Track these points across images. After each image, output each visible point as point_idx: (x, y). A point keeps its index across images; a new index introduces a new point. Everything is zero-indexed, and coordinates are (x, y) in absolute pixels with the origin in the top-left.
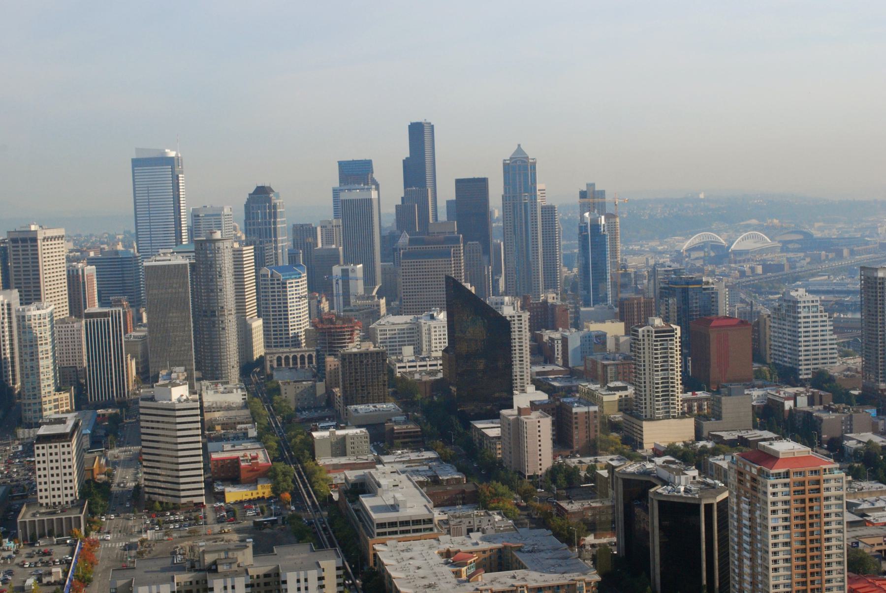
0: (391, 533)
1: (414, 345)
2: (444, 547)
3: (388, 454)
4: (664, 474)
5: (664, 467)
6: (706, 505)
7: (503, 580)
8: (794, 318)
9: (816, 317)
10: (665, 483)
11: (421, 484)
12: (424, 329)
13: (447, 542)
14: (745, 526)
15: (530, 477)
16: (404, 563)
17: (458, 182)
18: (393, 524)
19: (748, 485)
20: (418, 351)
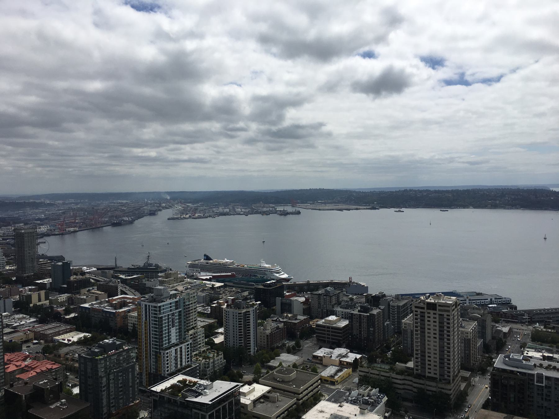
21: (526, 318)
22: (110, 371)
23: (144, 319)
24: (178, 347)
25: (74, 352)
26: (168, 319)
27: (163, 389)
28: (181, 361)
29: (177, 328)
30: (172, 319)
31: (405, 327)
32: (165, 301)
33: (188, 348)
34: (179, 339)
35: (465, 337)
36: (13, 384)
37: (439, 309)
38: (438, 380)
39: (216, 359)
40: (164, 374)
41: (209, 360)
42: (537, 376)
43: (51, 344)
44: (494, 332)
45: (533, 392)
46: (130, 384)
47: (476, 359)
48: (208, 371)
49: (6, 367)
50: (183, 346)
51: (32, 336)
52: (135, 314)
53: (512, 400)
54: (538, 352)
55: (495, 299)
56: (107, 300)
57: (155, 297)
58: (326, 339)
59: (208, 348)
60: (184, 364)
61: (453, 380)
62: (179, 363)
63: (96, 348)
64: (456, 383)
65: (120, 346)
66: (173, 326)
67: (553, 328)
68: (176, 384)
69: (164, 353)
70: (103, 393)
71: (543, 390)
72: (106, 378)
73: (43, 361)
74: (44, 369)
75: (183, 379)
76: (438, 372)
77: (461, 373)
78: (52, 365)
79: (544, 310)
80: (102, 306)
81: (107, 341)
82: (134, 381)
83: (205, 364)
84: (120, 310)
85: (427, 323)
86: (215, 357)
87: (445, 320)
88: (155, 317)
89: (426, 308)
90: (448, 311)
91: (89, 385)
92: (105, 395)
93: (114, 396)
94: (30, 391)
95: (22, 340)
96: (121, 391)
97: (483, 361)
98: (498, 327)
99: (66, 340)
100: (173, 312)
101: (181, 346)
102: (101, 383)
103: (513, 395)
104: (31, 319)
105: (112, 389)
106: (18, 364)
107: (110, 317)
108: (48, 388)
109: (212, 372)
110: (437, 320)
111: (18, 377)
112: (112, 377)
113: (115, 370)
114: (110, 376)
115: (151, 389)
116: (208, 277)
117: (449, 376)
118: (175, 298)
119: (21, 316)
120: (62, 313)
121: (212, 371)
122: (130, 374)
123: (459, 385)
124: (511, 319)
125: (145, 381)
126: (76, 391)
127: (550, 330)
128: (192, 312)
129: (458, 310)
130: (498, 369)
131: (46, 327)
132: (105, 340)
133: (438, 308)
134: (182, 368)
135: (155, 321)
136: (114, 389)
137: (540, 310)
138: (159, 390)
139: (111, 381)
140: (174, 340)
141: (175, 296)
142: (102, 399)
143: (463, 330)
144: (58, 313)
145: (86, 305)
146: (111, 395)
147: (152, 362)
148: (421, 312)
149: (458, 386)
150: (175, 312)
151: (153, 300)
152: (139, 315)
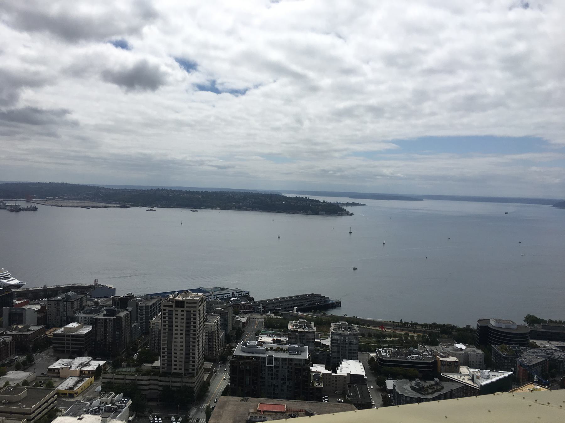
21: (261, 308)
31: (153, 327)
35: (209, 330)
37: (186, 306)
38: (183, 375)
42: (268, 358)
44: (234, 323)
45: (264, 373)
47: (218, 350)
53: (248, 383)
54: (269, 337)
55: (236, 293)
61: (197, 373)
64: (199, 375)
67: (282, 315)
71: (272, 370)
76: (183, 368)
77: (205, 365)
79: (275, 299)
85: (174, 320)
87: (192, 316)
89: (174, 306)
90: (195, 307)
97: (224, 351)
98: (238, 318)
103: (248, 379)
110: (184, 317)
117: (193, 370)
123: (202, 377)
124: (248, 310)
127: (279, 317)
129: (204, 305)
130: (237, 356)
133: (186, 305)
137: (272, 300)
143: (208, 324)
148: (170, 311)
149: (201, 378)
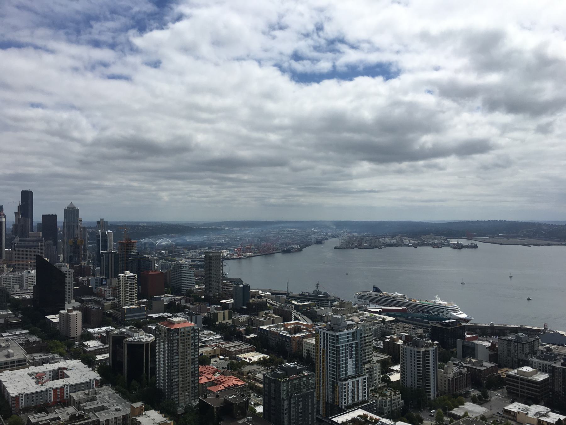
0: (5, 368)
1: (19, 284)
2: (30, 372)
3: (5, 332)
4: (130, 333)
5: (129, 330)
6: (146, 344)
7: (57, 383)
8: (180, 270)
9: (188, 270)
10: (131, 337)
11: (21, 345)
12: (25, 277)
13: (33, 369)
14: (162, 351)
15: (71, 338)
16: (11, 381)
17: (44, 216)
18: (6, 363)
19: (163, 335)
20: (21, 287)
22: (292, 395)
23: (322, 347)
24: (355, 380)
25: (256, 372)
26: (346, 349)
27: (344, 421)
28: (358, 395)
29: (354, 359)
30: (350, 350)
32: (342, 331)
33: (365, 382)
34: (356, 371)
36: (207, 395)
39: (393, 397)
40: (341, 406)
41: (387, 398)
43: (235, 361)
46: (310, 412)
48: (385, 410)
49: (200, 378)
50: (360, 379)
51: (218, 352)
52: (313, 341)
56: (283, 324)
57: (332, 326)
58: (519, 393)
59: (384, 385)
60: (360, 398)
62: (356, 396)
63: (279, 370)
65: (300, 372)
66: (350, 357)
68: (356, 418)
69: (341, 384)
70: (285, 416)
72: (288, 401)
73: (230, 376)
74: (231, 384)
75: (364, 414)
78: (238, 382)
80: (279, 329)
81: (289, 364)
82: (313, 408)
83: (382, 402)
84: (296, 336)
86: (392, 396)
88: (333, 346)
91: (273, 406)
92: (287, 418)
93: (294, 421)
94: (222, 404)
95: (210, 355)
96: (301, 417)
99: (248, 359)
100: (350, 343)
101: (357, 379)
102: (283, 405)
104: (217, 335)
105: (293, 414)
106: (209, 376)
107: (286, 341)
108: (237, 404)
109: (389, 411)
111: (209, 389)
112: (293, 401)
113: (296, 395)
114: (292, 399)
115: (332, 419)
116: (378, 310)
118: (353, 329)
119: (209, 332)
120: (244, 332)
121: (390, 410)
122: (310, 400)
125: (322, 410)
126: (260, 409)
128: (368, 345)
131: (230, 345)
132: (287, 364)
134: (358, 402)
135: (333, 350)
136: (294, 413)
138: (340, 422)
139: (292, 405)
140: (351, 372)
141: (351, 326)
142: (284, 422)
144: (240, 332)
145: (265, 327)
146: (292, 419)
147: (329, 391)
150: (352, 343)
151: (331, 329)
152: (317, 342)
